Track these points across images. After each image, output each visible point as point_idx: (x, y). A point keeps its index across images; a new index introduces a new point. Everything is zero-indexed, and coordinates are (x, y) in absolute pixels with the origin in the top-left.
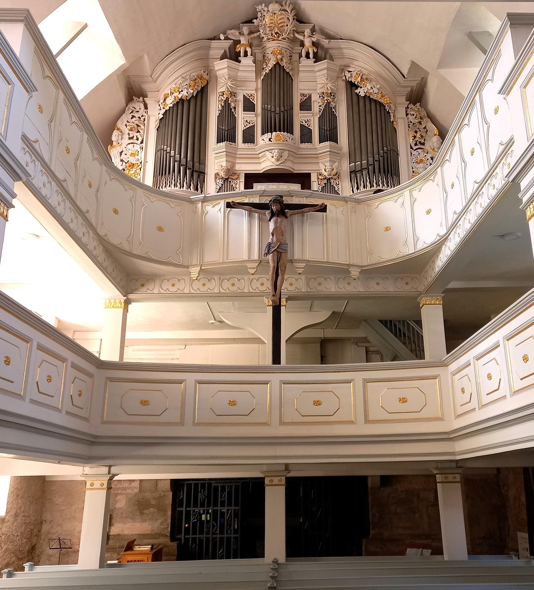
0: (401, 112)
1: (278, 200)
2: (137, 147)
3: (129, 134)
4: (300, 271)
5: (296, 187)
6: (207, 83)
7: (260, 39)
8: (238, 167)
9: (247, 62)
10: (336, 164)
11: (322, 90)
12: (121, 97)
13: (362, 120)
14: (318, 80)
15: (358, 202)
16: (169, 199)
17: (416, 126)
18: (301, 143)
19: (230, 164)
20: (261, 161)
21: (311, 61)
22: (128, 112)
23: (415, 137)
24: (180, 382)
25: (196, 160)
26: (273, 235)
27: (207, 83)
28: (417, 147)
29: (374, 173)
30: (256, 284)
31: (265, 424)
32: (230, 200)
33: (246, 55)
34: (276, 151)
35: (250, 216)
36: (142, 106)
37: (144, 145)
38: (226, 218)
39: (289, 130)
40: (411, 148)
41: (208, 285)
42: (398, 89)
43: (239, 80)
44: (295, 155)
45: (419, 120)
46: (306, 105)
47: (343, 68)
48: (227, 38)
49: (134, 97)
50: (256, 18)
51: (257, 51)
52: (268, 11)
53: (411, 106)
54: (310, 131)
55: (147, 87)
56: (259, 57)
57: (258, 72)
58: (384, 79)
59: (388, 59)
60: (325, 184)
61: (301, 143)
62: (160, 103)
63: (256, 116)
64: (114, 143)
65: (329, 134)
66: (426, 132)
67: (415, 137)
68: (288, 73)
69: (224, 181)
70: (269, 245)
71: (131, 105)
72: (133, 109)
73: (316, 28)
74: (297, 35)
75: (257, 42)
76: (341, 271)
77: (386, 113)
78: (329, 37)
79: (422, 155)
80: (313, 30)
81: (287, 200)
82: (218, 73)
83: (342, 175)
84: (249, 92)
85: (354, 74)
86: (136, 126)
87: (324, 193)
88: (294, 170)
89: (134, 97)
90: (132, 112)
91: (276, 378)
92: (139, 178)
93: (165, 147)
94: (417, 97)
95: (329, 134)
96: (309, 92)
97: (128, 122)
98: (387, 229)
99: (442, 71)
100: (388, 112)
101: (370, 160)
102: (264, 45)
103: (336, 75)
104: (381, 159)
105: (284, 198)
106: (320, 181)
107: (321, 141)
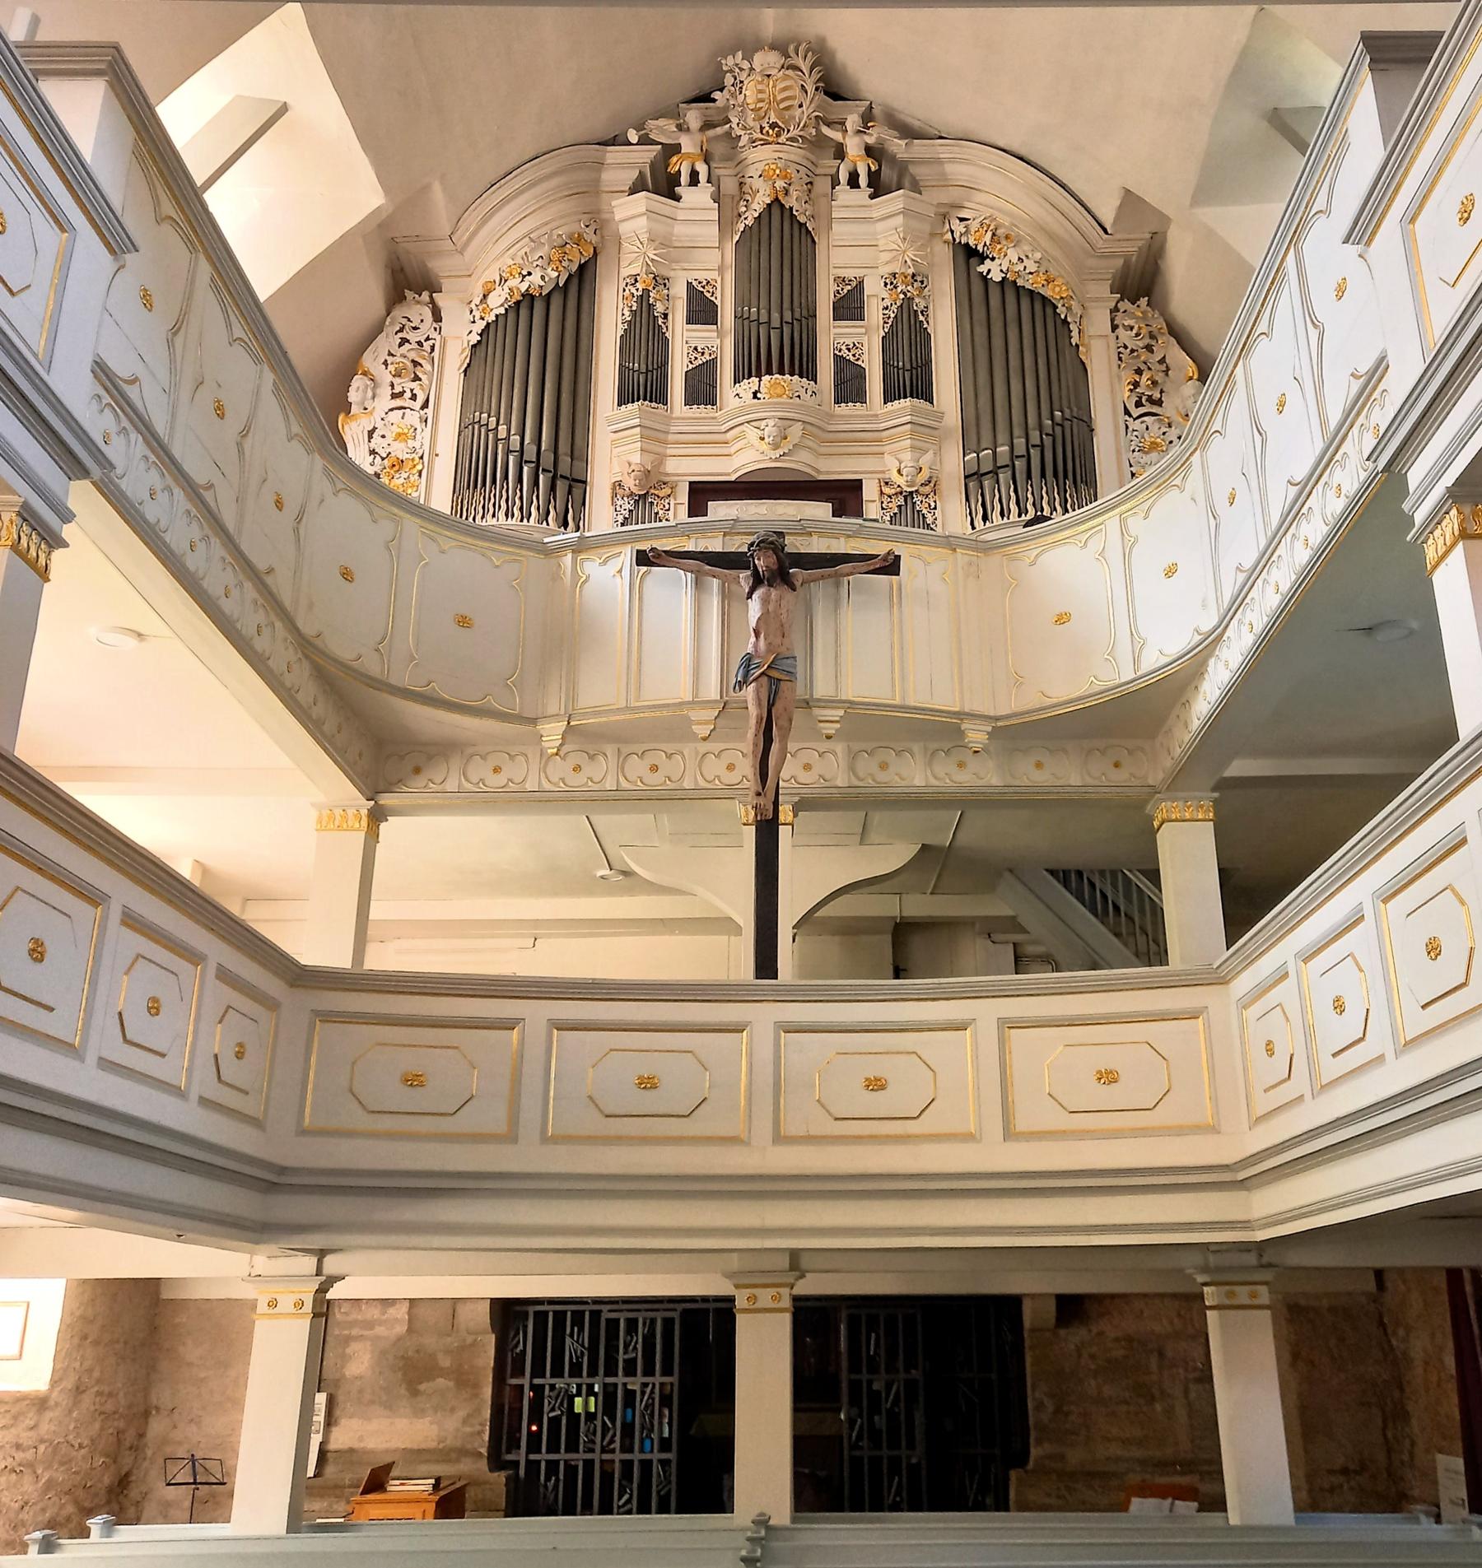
0: (1099, 321)
1: (772, 543)
2: (413, 418)
3: (392, 385)
4: (830, 729)
5: (820, 510)
6: (595, 254)
7: (732, 139)
8: (672, 466)
9: (698, 199)
10: (929, 456)
11: (889, 269)
12: (371, 291)
13: (998, 342)
14: (880, 243)
15: (987, 548)
16: (486, 544)
17: (1138, 357)
18: (837, 402)
19: (649, 458)
20: (732, 450)
21: (865, 191)
22: (391, 328)
23: (1136, 384)
24: (508, 1025)
25: (564, 447)
26: (757, 635)
27: (595, 254)
28: (1142, 410)
29: (1029, 477)
30: (715, 768)
31: (733, 1140)
32: (645, 546)
33: (694, 180)
34: (771, 423)
35: (698, 584)
36: (427, 313)
37: (429, 411)
38: (636, 591)
39: (806, 369)
40: (1127, 412)
41: (589, 770)
42: (1092, 262)
43: (676, 244)
44: (818, 432)
45: (1147, 341)
46: (850, 306)
47: (942, 210)
48: (645, 141)
49: (407, 293)
50: (721, 90)
51: (724, 172)
52: (752, 69)
53: (1125, 305)
54: (860, 374)
55: (440, 266)
56: (729, 186)
57: (724, 225)
58: (1052, 236)
59: (1063, 186)
60: (900, 507)
61: (837, 402)
62: (473, 306)
63: (721, 335)
64: (354, 409)
65: (910, 379)
66: (1166, 372)
67: (1136, 384)
68: (802, 225)
69: (636, 502)
70: (748, 662)
71: (398, 313)
72: (404, 321)
73: (877, 111)
74: (825, 130)
75: (723, 150)
76: (940, 731)
77: (1059, 322)
78: (909, 133)
79: (1155, 430)
80: (868, 117)
81: (795, 544)
82: (625, 229)
83: (944, 486)
84: (702, 276)
85: (974, 225)
86: (410, 365)
87: (898, 527)
88: (818, 471)
89: (407, 293)
90: (401, 330)
91: (763, 1016)
92: (417, 495)
93: (485, 415)
94: (1141, 282)
95: (910, 379)
96: (859, 273)
97: (390, 354)
98: (1062, 619)
99: (1209, 215)
100: (1065, 322)
101: (1020, 442)
102: (743, 156)
103: (927, 228)
104: (1048, 441)
105: (788, 540)
106: (886, 499)
107: (888, 397)
